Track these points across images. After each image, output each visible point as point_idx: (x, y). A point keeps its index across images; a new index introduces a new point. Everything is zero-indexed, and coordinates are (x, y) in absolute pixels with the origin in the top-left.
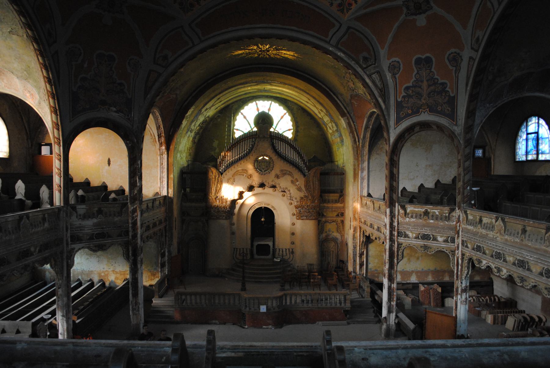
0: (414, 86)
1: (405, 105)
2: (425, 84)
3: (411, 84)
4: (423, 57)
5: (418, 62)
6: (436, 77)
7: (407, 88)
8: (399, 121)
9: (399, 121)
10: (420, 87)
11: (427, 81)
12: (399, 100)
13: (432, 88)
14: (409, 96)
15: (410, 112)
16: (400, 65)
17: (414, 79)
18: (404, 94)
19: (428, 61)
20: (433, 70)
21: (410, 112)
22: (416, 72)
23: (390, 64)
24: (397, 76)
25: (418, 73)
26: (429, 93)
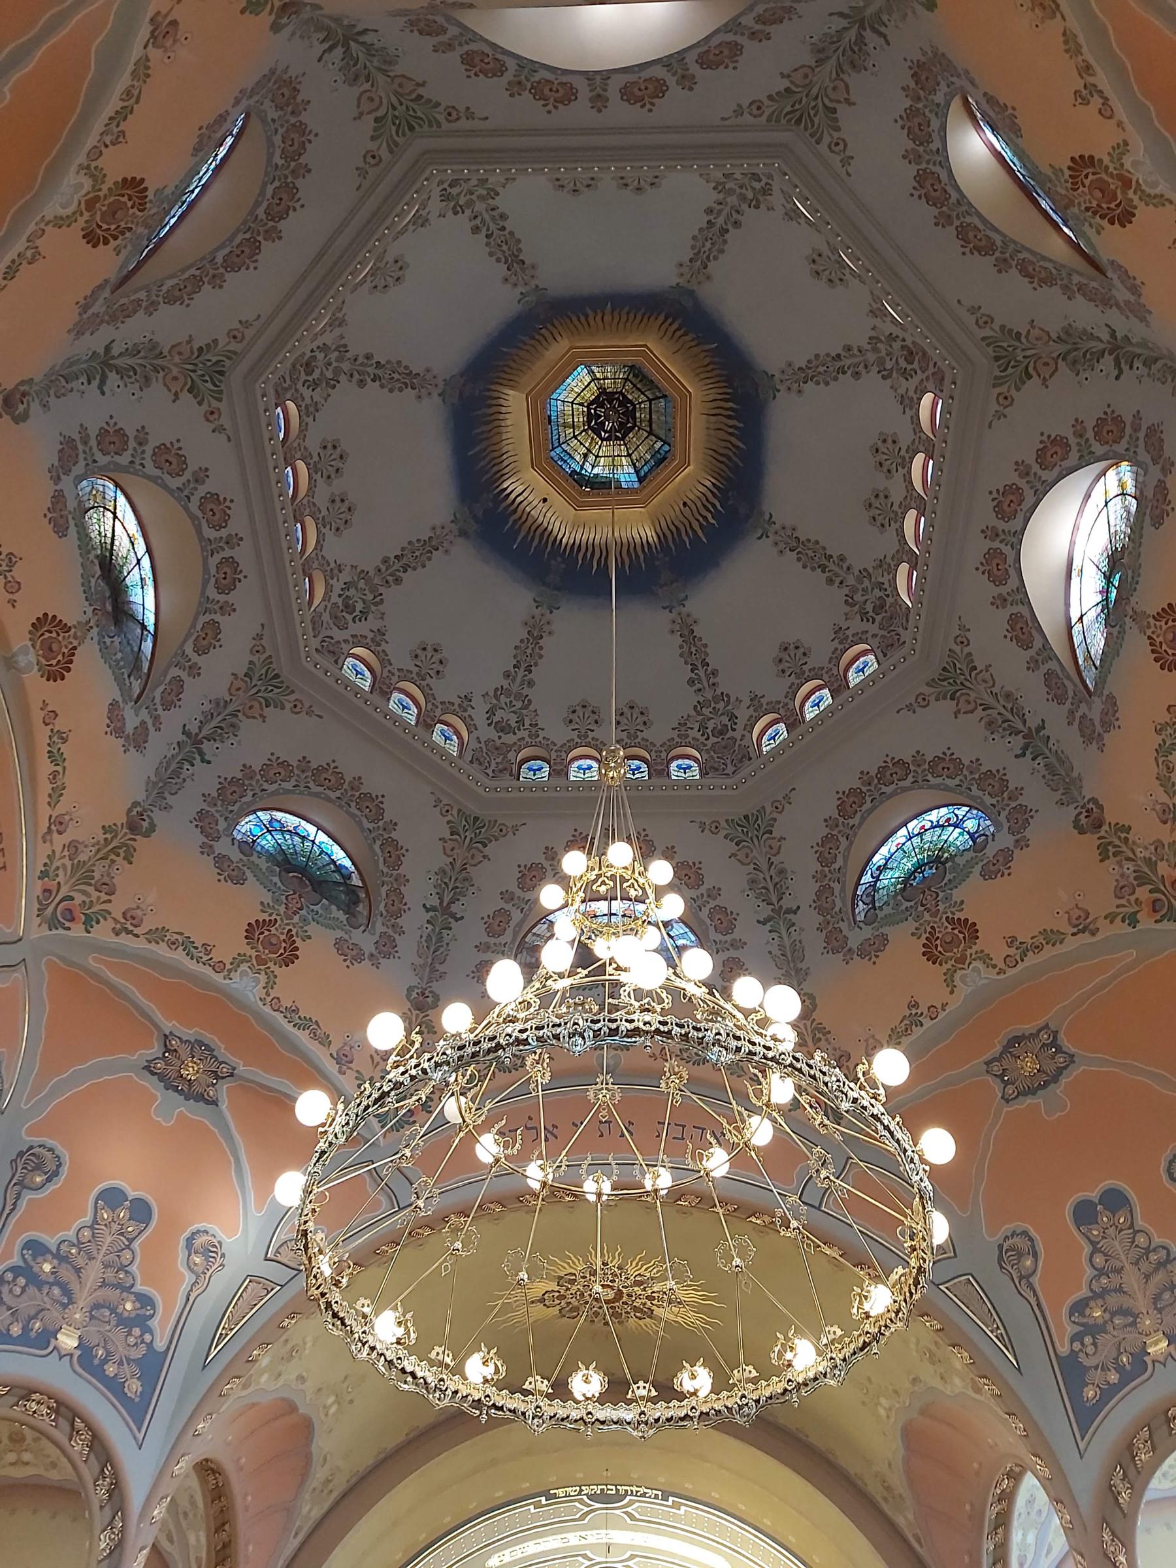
0: (1096, 1296)
1: (1087, 1363)
2: (1131, 1278)
3: (1084, 1292)
4: (1094, 1195)
5: (1085, 1214)
6: (1157, 1240)
7: (1080, 1307)
8: (1085, 1418)
9: (1085, 1418)
10: (1120, 1290)
11: (1136, 1263)
12: (1064, 1350)
13: (1159, 1277)
14: (1095, 1330)
15: (1113, 1377)
16: (1031, 1240)
17: (1089, 1272)
18: (1070, 1329)
19: (1115, 1200)
20: (1140, 1223)
21: (1113, 1377)
22: (1087, 1249)
23: (1000, 1247)
24: (1035, 1280)
25: (1095, 1250)
26: (1157, 1298)
